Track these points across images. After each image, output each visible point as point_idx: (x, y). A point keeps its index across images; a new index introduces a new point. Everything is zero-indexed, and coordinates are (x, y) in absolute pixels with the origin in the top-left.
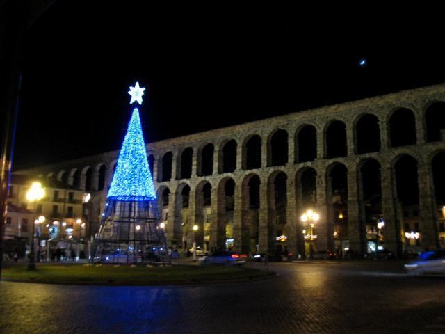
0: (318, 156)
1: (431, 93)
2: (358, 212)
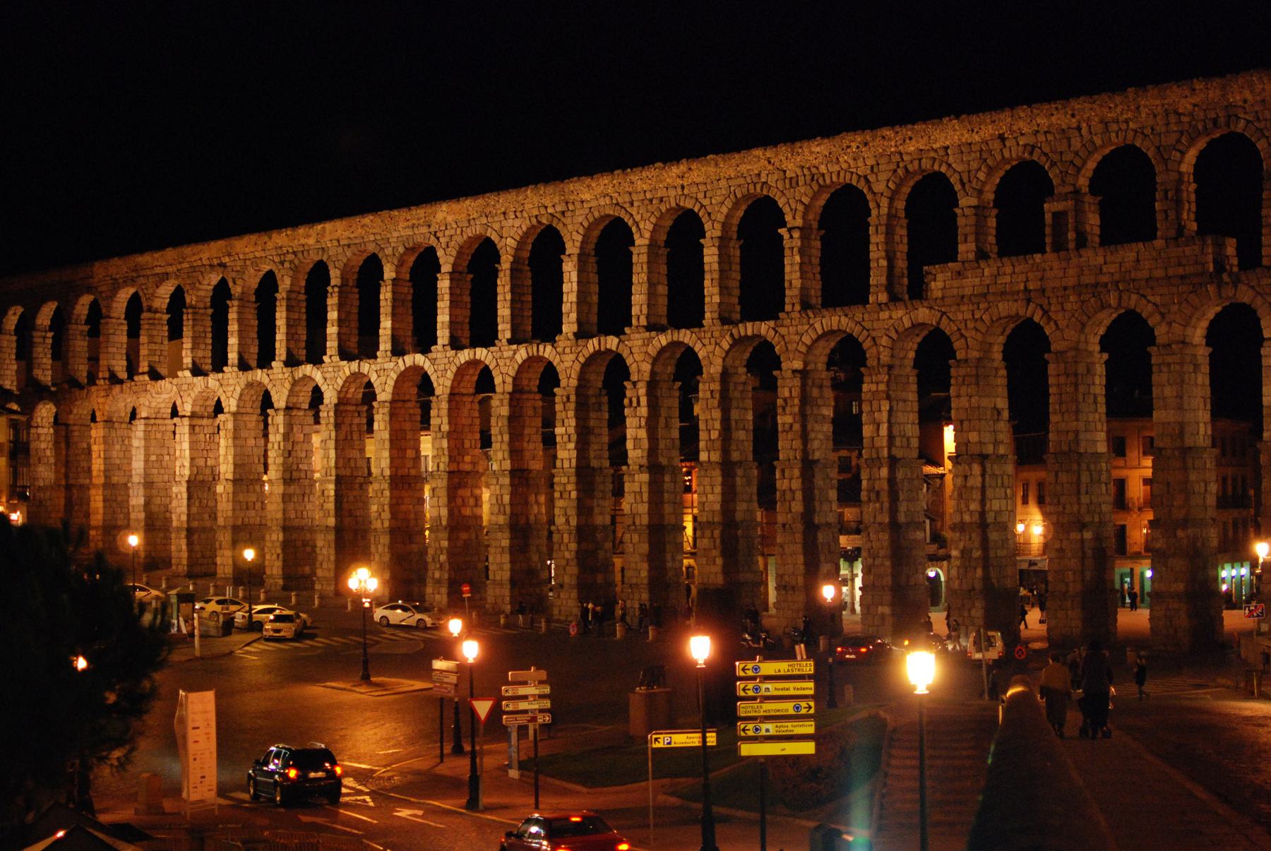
0: (634, 322)
1: (911, 147)
2: (719, 498)
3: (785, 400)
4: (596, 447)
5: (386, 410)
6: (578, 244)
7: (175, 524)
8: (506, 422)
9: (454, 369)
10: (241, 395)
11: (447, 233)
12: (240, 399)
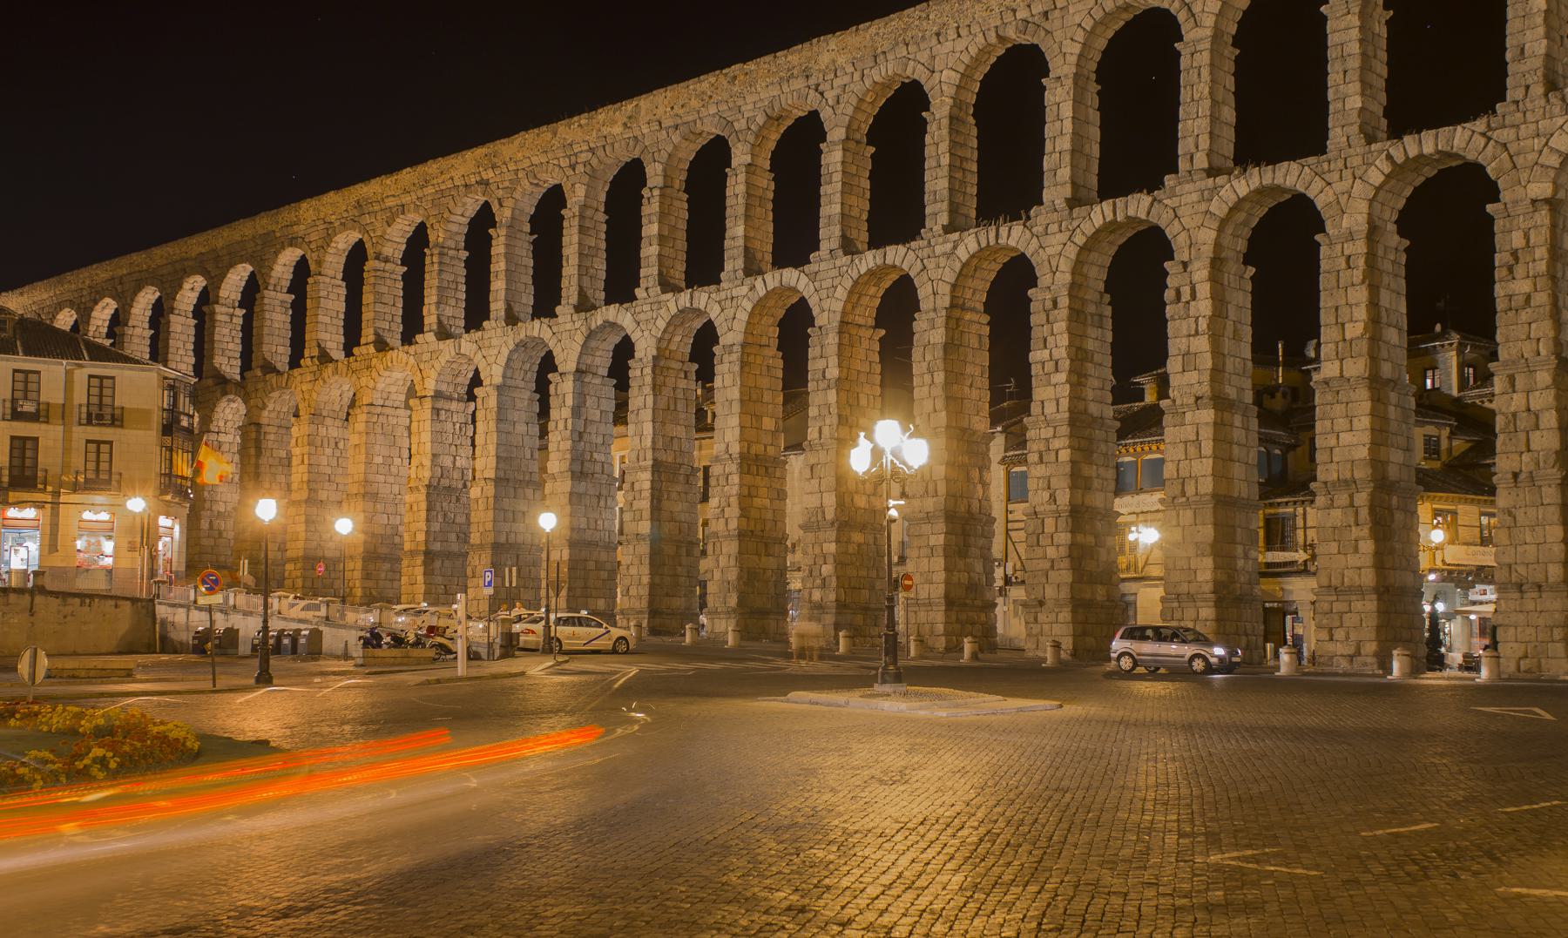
0: (1182, 164)
2: (1366, 438)
3: (1515, 254)
4: (1096, 383)
5: (735, 357)
6: (1073, 59)
7: (407, 546)
8: (939, 353)
9: (848, 284)
10: (509, 359)
11: (837, 82)
12: (507, 365)
